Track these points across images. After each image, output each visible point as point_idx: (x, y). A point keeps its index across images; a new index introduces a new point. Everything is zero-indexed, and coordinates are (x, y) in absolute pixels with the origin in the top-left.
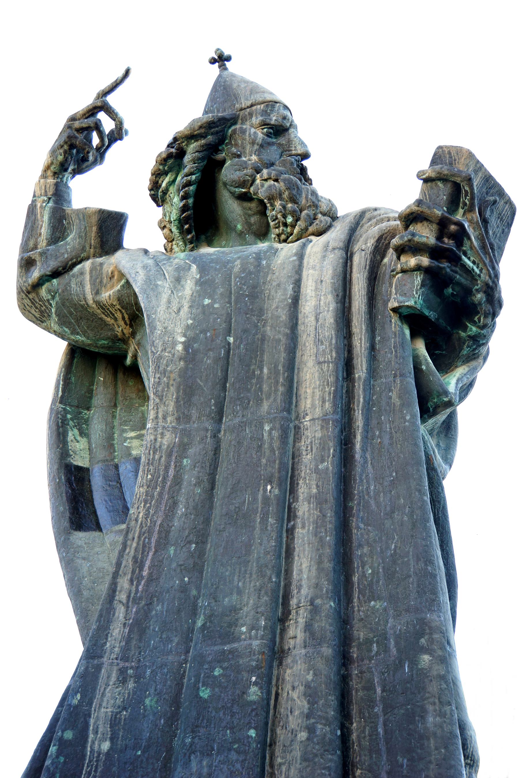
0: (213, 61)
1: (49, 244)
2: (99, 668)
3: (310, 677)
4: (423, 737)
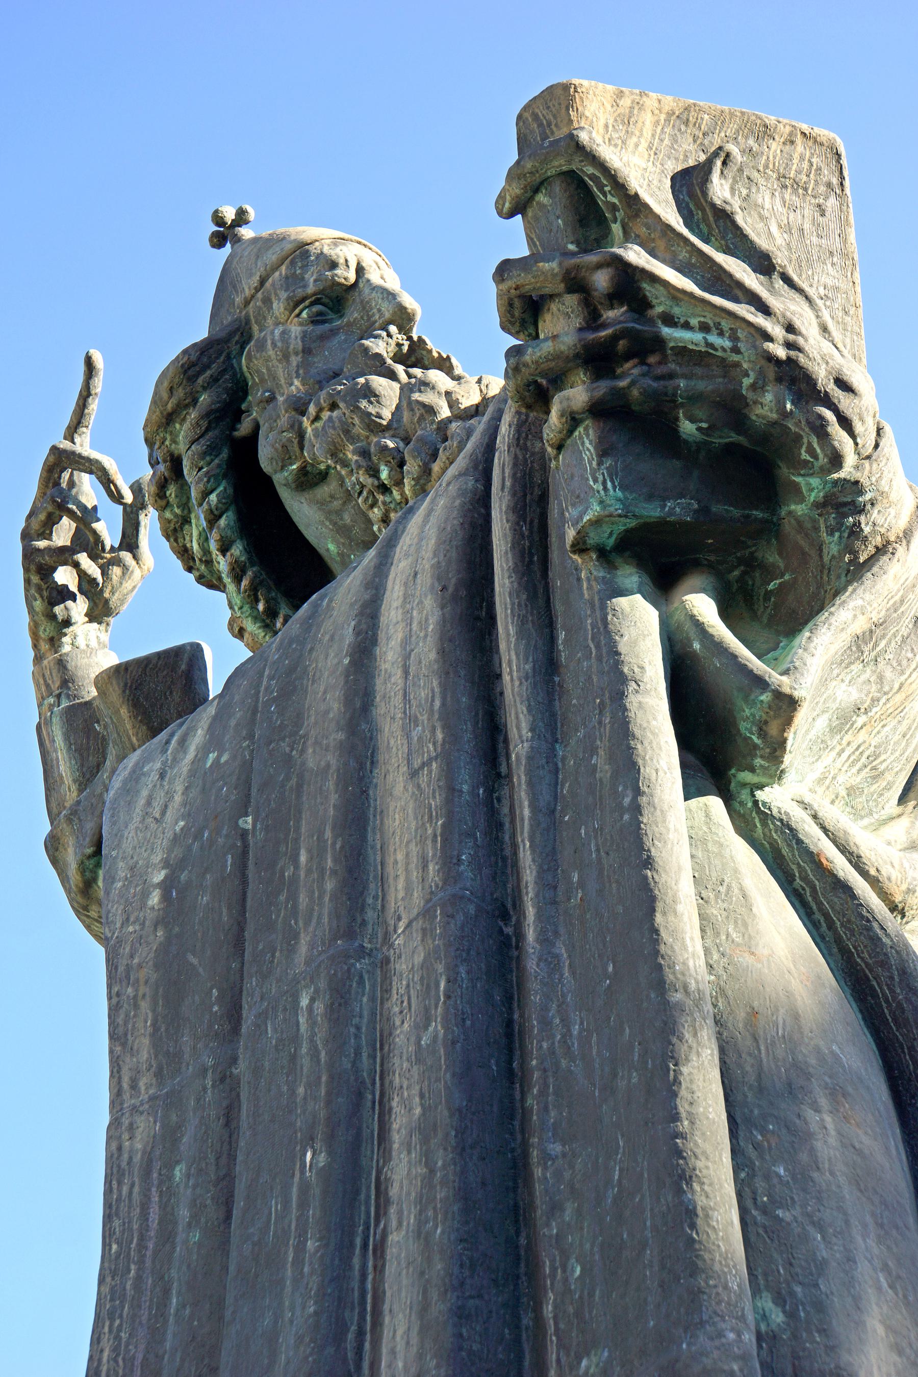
1: (81, 791)
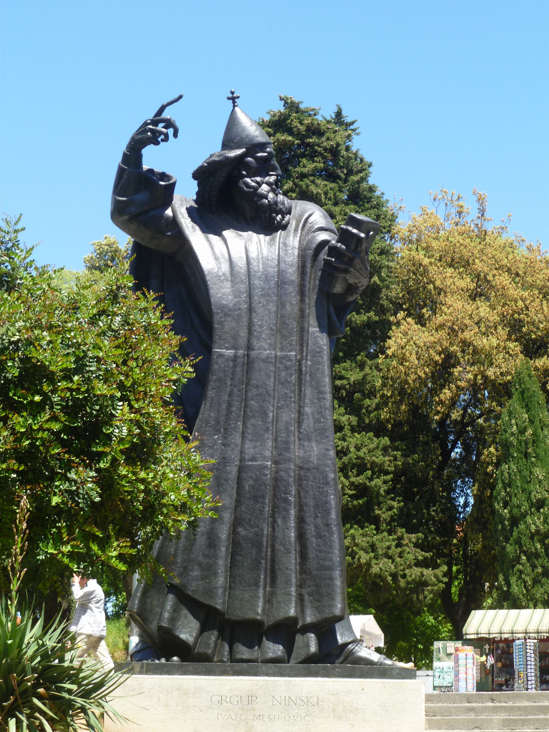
0: (229, 99)
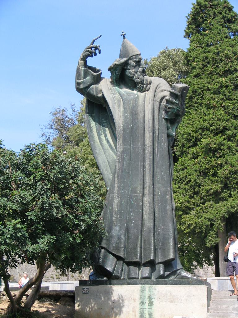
0: (122, 35)
2: (114, 196)
3: (149, 200)
4: (167, 210)
